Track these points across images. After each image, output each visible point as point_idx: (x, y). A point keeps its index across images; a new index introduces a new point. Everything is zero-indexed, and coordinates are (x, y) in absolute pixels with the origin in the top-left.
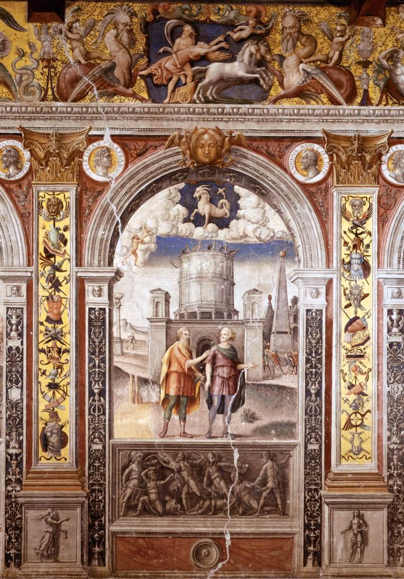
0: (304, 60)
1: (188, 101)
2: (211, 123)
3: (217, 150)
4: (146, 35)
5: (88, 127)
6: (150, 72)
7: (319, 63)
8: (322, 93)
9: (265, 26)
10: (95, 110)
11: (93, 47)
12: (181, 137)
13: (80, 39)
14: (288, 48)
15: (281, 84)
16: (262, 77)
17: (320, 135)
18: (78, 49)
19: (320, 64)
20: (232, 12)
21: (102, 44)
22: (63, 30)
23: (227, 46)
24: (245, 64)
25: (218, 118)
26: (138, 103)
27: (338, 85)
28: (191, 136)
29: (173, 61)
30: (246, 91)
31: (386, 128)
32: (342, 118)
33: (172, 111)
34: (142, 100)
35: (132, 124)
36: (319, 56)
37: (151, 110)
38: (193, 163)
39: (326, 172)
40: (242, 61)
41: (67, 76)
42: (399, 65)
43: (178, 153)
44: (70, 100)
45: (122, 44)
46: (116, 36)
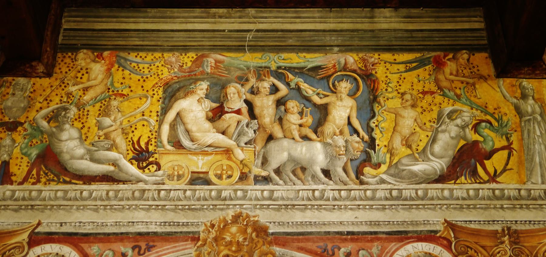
31: (28, 219)
42: (67, 126)
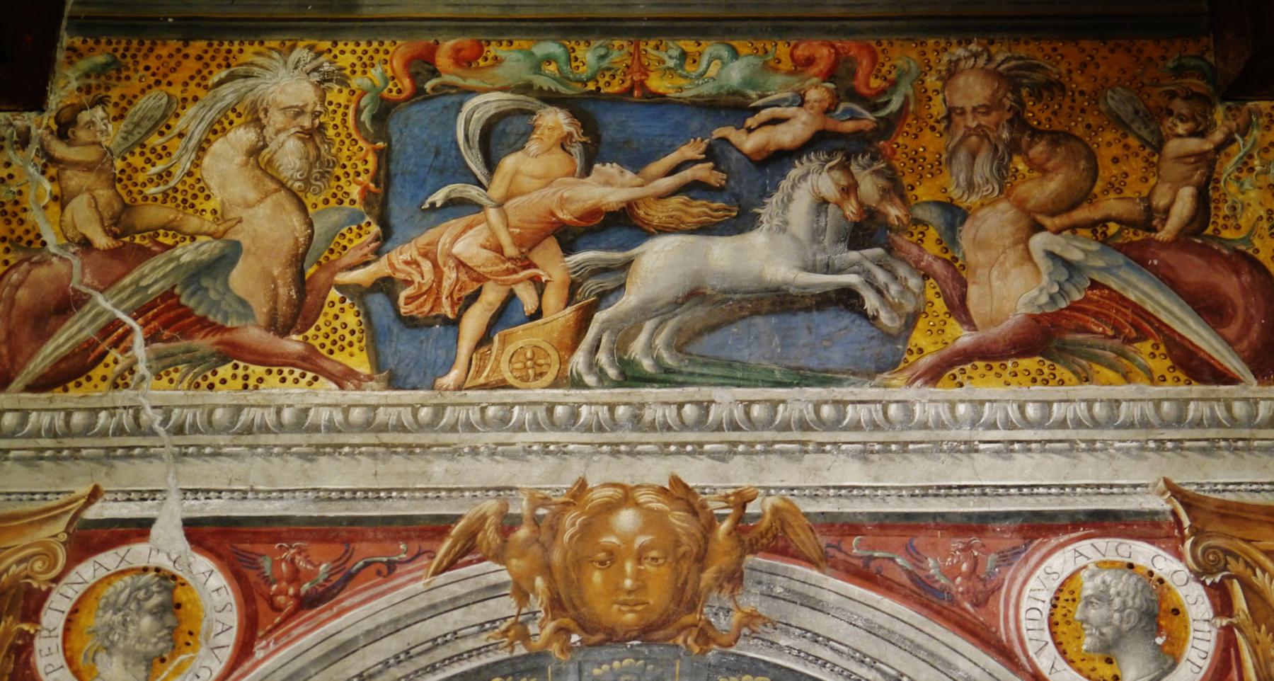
0: (1047, 222)
1: (549, 378)
2: (649, 461)
3: (676, 572)
4: (380, 144)
5: (87, 489)
6: (388, 272)
7: (1113, 228)
8: (1143, 336)
9: (874, 108)
10: (127, 419)
11: (151, 190)
12: (508, 525)
13: (100, 161)
14: (977, 179)
15: (959, 309)
16: (871, 283)
17: (1157, 503)
18: (83, 199)
19: (1119, 233)
20: (736, 64)
21: (190, 181)
22: (34, 132)
23: (716, 178)
24: (794, 238)
25: (683, 444)
26: (326, 390)
27: (1211, 309)
28: (558, 516)
29: (486, 233)
30: (804, 338)
32: (1245, 433)
33: (475, 416)
34: (344, 378)
35: (289, 473)
36: (1112, 205)
37: (382, 415)
38: (563, 631)
39: (1206, 665)
40: (784, 227)
41: (22, 294)
43: (494, 590)
44: (19, 383)
45: (273, 178)
46: (254, 152)
